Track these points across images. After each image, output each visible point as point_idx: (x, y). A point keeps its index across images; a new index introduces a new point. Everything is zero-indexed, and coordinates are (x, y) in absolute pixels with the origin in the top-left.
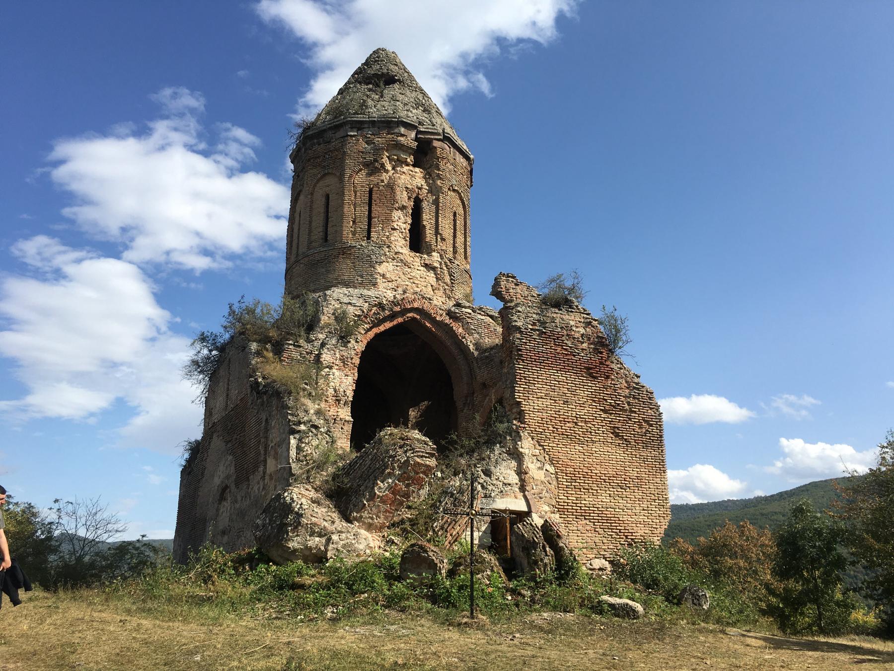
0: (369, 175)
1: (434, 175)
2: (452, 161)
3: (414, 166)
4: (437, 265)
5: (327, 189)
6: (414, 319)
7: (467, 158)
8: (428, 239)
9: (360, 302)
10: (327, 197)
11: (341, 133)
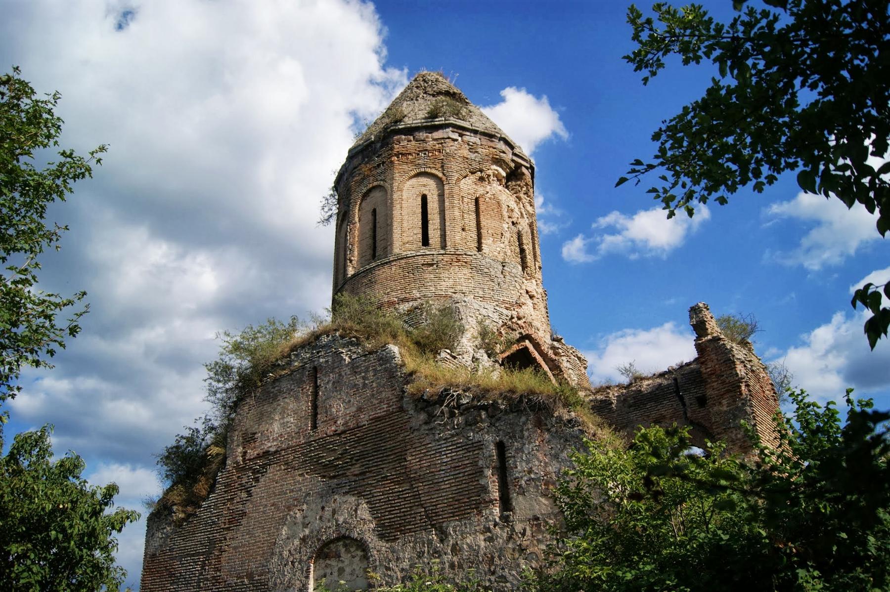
1: (524, 200)
4: (534, 293)
5: (423, 189)
6: (526, 348)
9: (495, 317)
10: (424, 198)
11: (438, 134)
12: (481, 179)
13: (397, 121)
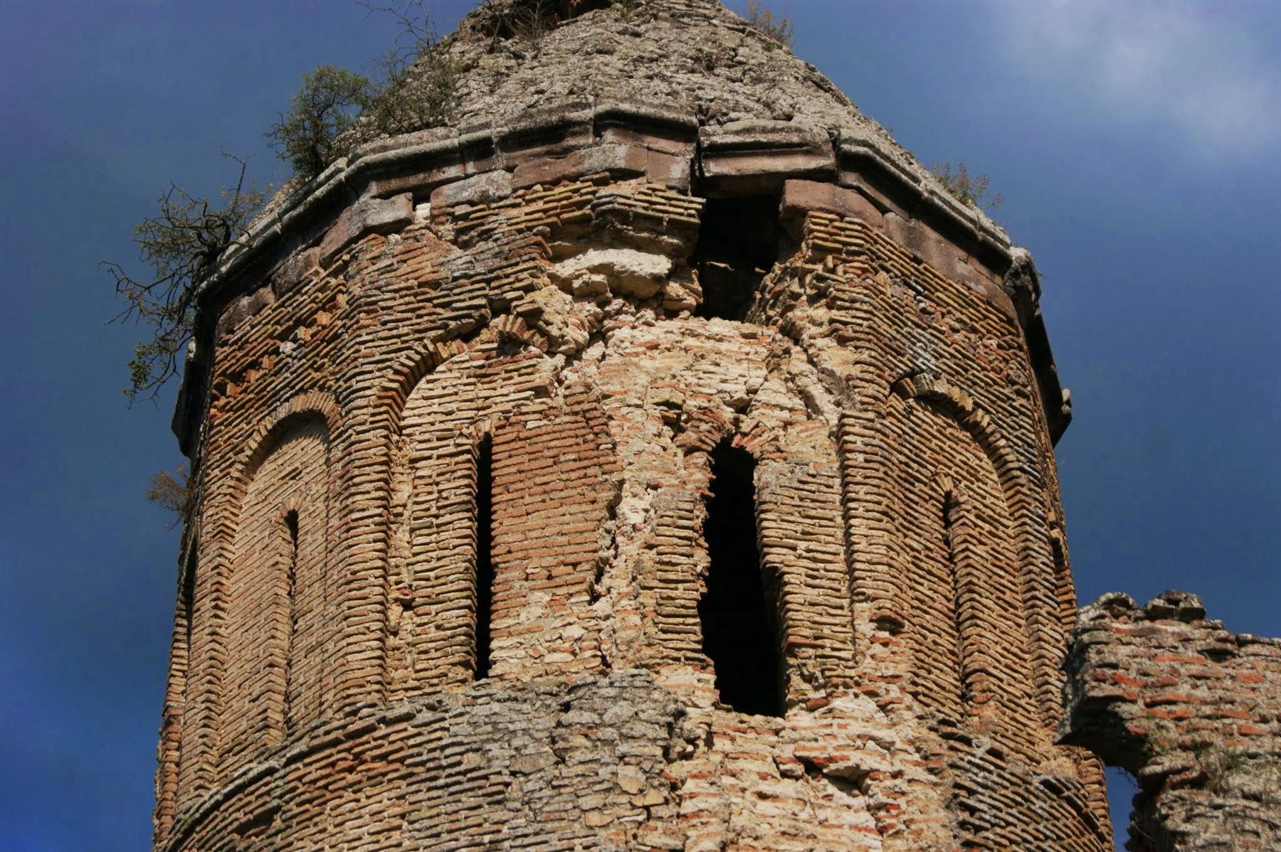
0: (482, 376)
2: (896, 263)
3: (704, 311)
4: (868, 760)
7: (993, 258)
8: (800, 632)
12: (509, 345)
13: (211, 256)
